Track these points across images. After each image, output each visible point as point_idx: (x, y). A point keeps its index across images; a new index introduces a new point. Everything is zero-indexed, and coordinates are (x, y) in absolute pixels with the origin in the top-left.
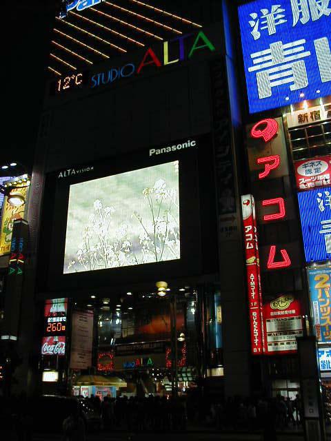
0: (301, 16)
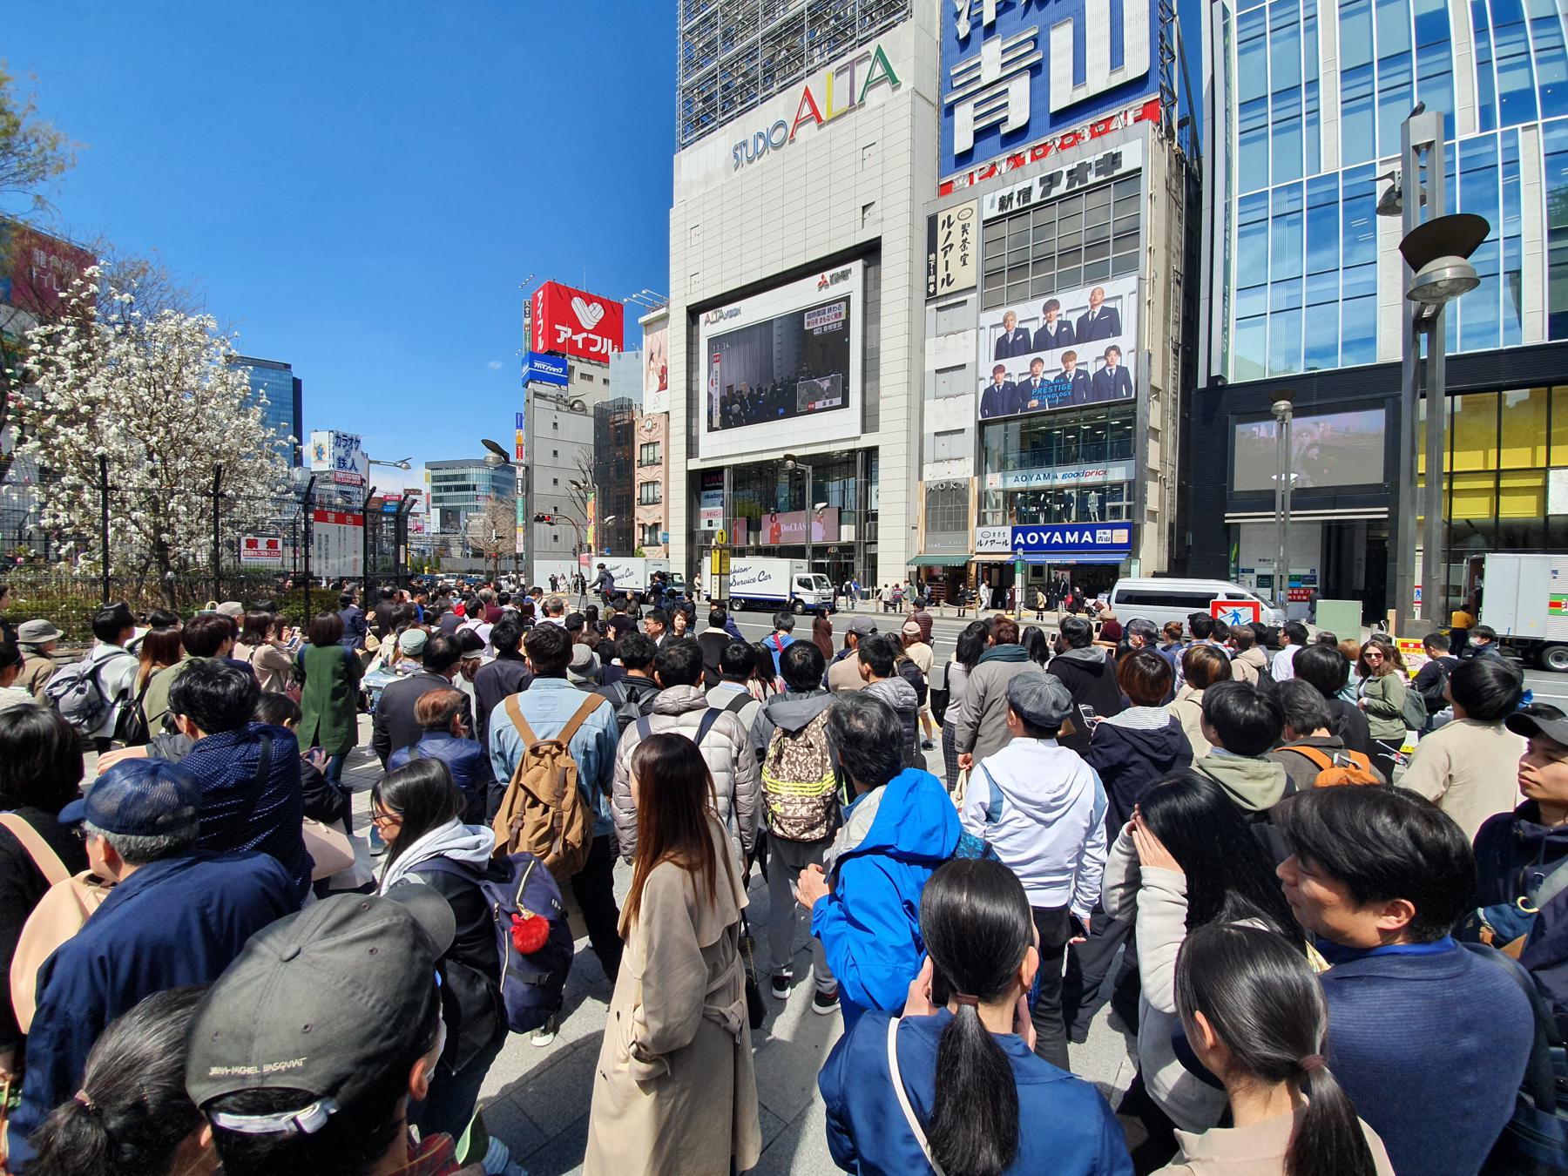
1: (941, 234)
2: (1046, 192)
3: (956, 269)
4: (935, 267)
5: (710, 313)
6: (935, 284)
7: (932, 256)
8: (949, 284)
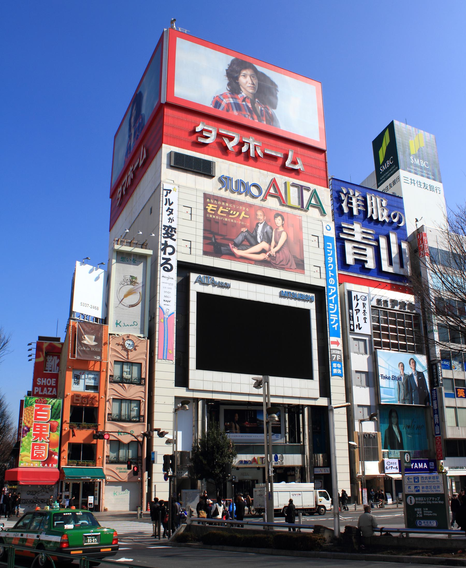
0: (373, 212)
1: (354, 303)
2: (393, 306)
3: (361, 322)
4: (353, 317)
5: (202, 276)
6: (353, 325)
7: (351, 311)
8: (360, 329)
